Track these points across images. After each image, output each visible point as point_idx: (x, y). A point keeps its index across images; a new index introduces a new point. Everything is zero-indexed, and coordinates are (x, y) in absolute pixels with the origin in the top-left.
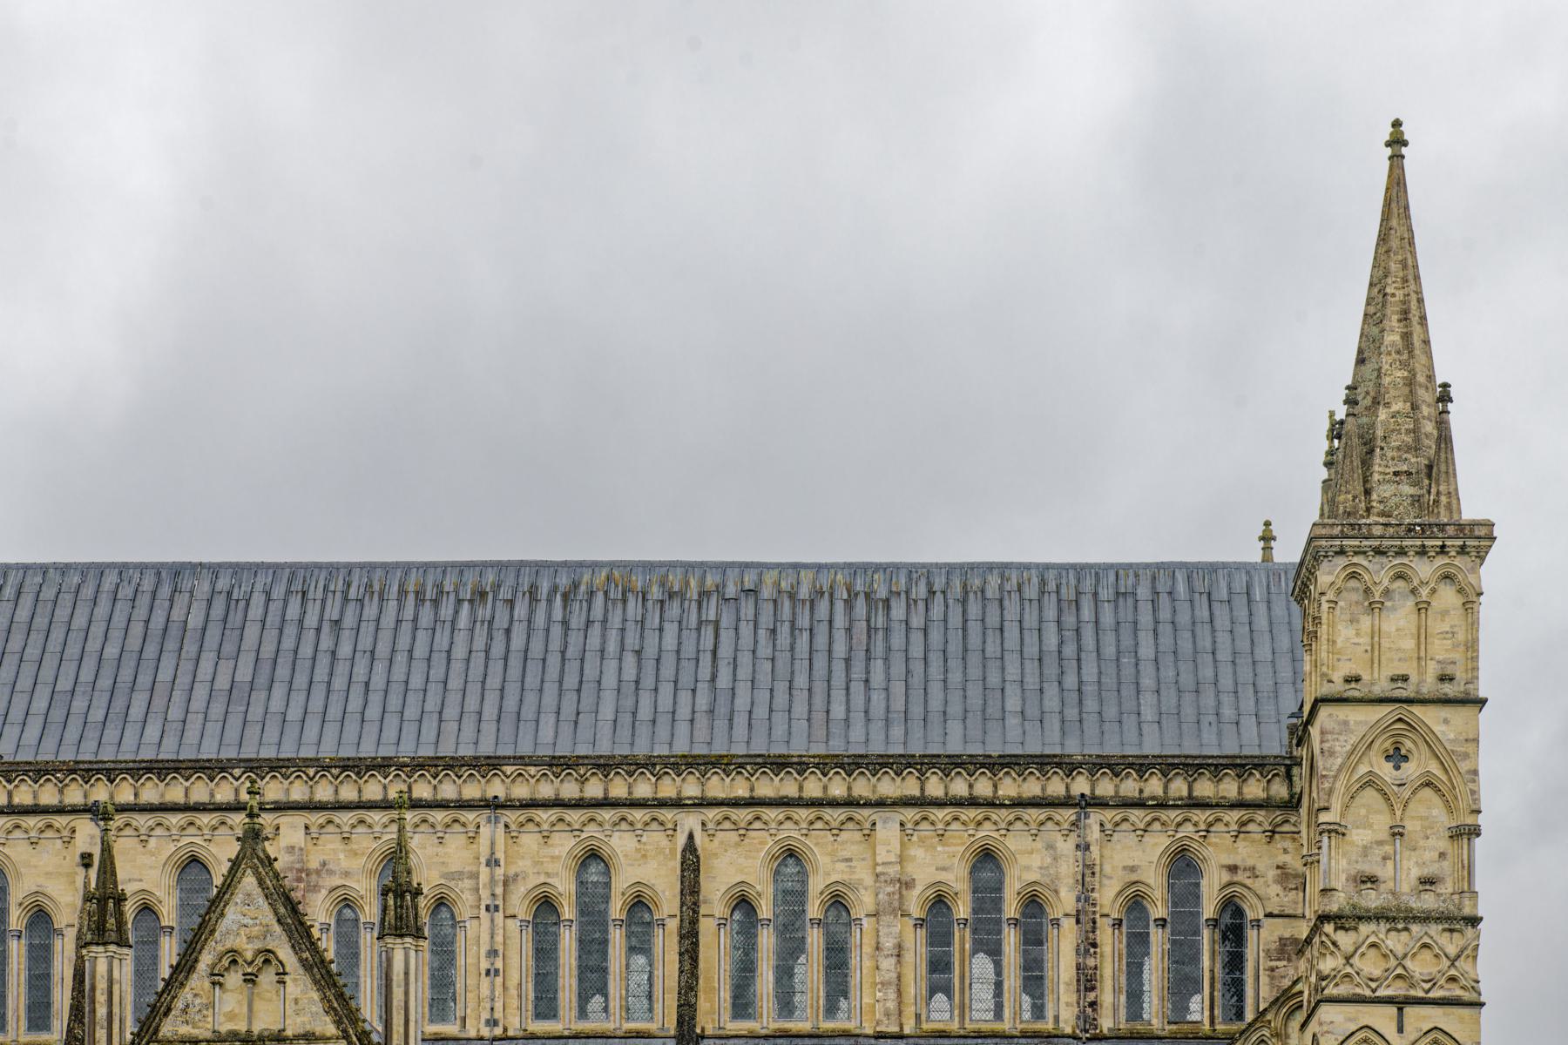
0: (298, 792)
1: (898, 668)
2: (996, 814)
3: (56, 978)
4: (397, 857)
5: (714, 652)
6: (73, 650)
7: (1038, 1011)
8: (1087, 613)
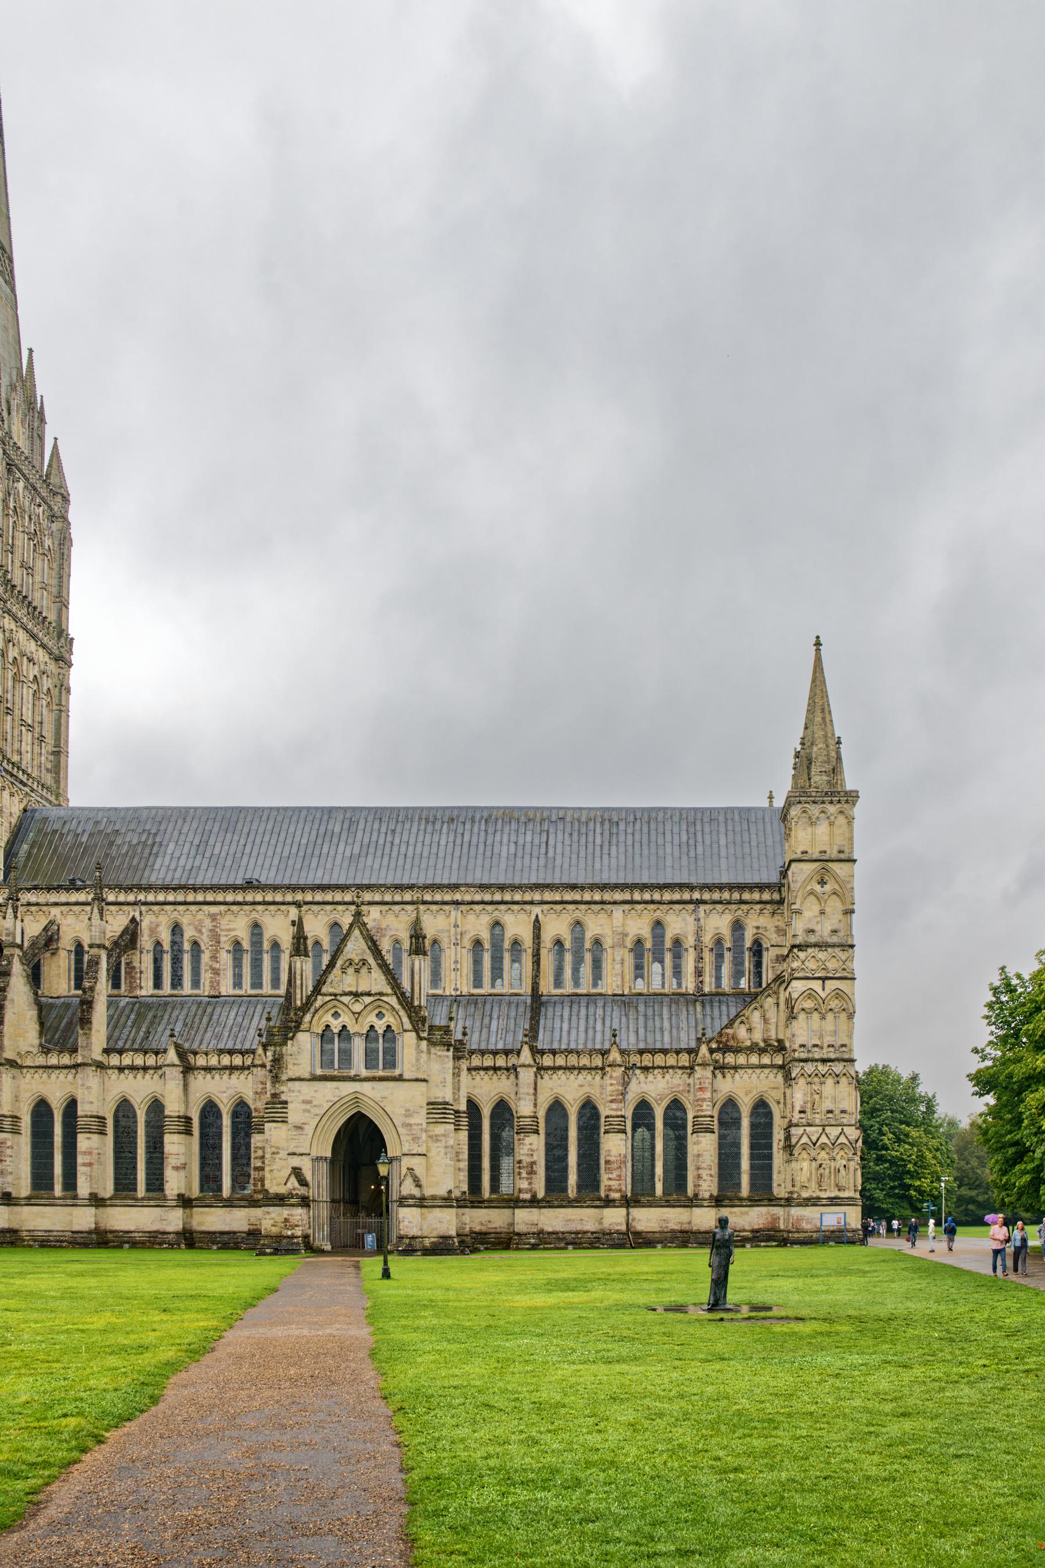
0: (377, 898)
1: (622, 849)
2: (661, 907)
3: (282, 969)
4: (416, 925)
5: (547, 843)
6: (289, 841)
7: (679, 985)
8: (699, 827)
